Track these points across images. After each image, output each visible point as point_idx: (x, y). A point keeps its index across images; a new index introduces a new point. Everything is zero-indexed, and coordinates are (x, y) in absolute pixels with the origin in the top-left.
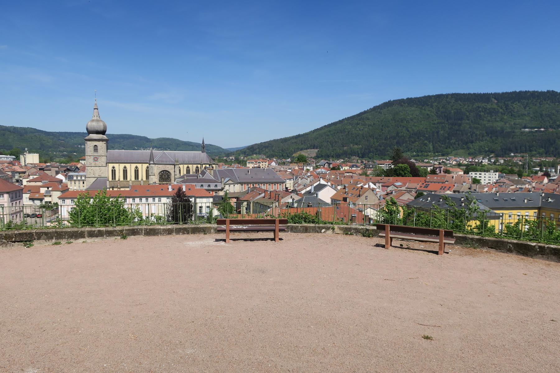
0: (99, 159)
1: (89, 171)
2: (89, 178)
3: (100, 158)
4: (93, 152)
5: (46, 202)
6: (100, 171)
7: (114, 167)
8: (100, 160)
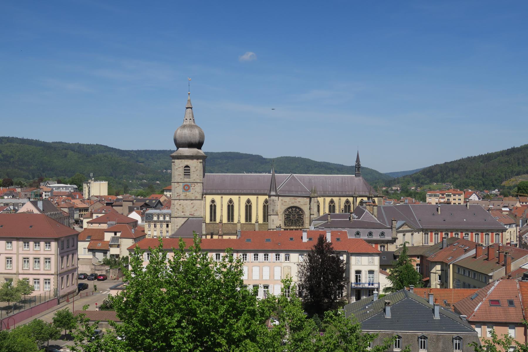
0: (191, 188)
1: (176, 207)
2: (176, 218)
3: (194, 185)
4: (182, 176)
6: (193, 207)
7: (213, 201)
8: (192, 189)
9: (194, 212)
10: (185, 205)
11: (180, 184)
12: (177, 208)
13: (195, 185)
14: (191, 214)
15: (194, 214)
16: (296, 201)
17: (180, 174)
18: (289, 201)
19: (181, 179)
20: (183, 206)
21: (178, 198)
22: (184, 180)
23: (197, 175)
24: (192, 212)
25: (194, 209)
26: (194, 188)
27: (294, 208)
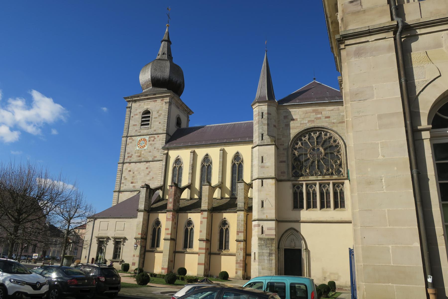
3: (153, 139)
5: (42, 262)
6: (148, 174)
8: (151, 144)
10: (137, 171)
13: (155, 138)
16: (319, 116)
17: (135, 124)
18: (303, 119)
19: (136, 131)
20: (134, 173)
22: (140, 132)
23: (160, 123)
26: (153, 142)
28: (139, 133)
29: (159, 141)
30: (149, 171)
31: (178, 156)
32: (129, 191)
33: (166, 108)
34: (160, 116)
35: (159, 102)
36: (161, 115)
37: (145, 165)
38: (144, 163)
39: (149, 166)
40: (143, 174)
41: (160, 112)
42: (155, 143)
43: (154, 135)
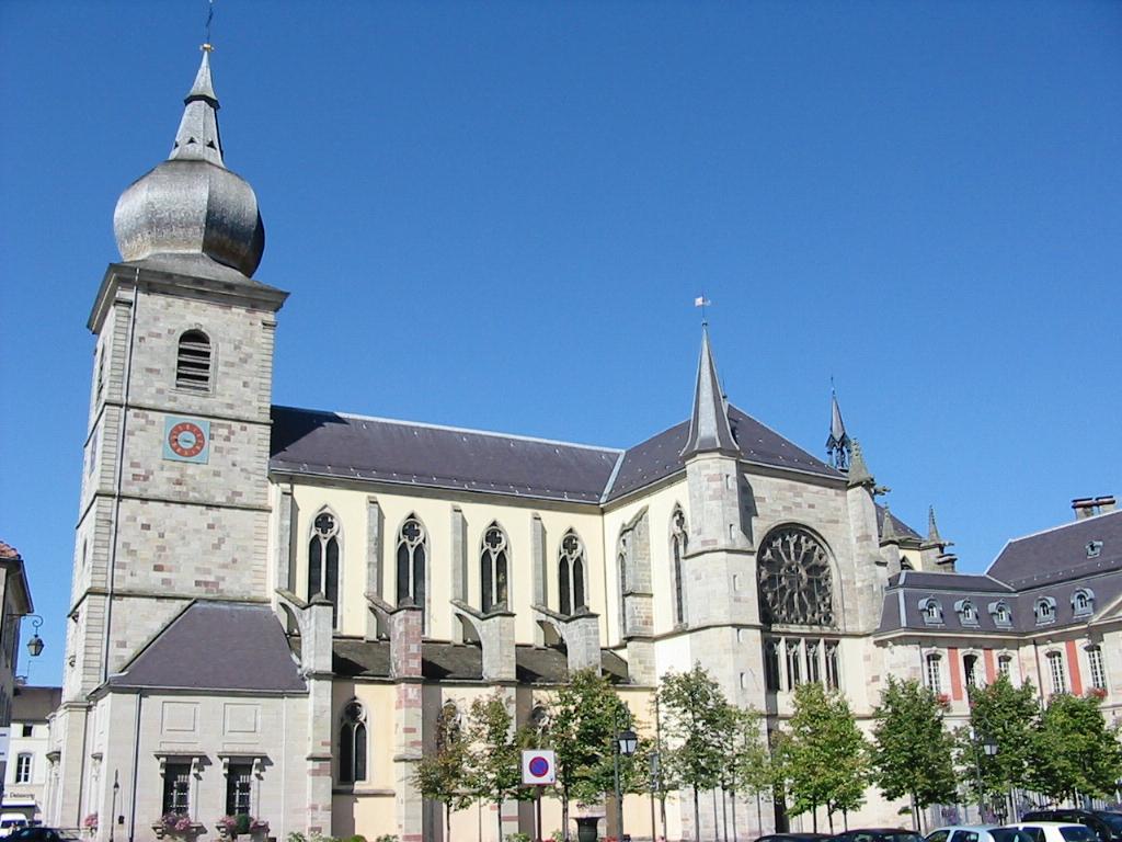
0: (210, 445)
3: (225, 432)
4: (169, 379)
6: (217, 547)
8: (218, 450)
9: (222, 572)
11: (151, 415)
12: (126, 545)
13: (232, 433)
14: (206, 584)
15: (222, 586)
17: (156, 367)
19: (160, 391)
20: (162, 536)
21: (134, 490)
22: (175, 399)
23: (245, 384)
24: (208, 572)
25: (217, 558)
27: (775, 539)
28: (170, 400)
29: (248, 443)
30: (219, 539)
31: (325, 506)
32: (151, 597)
33: (264, 340)
34: (246, 362)
35: (239, 314)
36: (249, 360)
37: (201, 513)
38: (200, 508)
39: (219, 520)
40: (195, 545)
41: (246, 349)
42: (233, 449)
43: (229, 422)
